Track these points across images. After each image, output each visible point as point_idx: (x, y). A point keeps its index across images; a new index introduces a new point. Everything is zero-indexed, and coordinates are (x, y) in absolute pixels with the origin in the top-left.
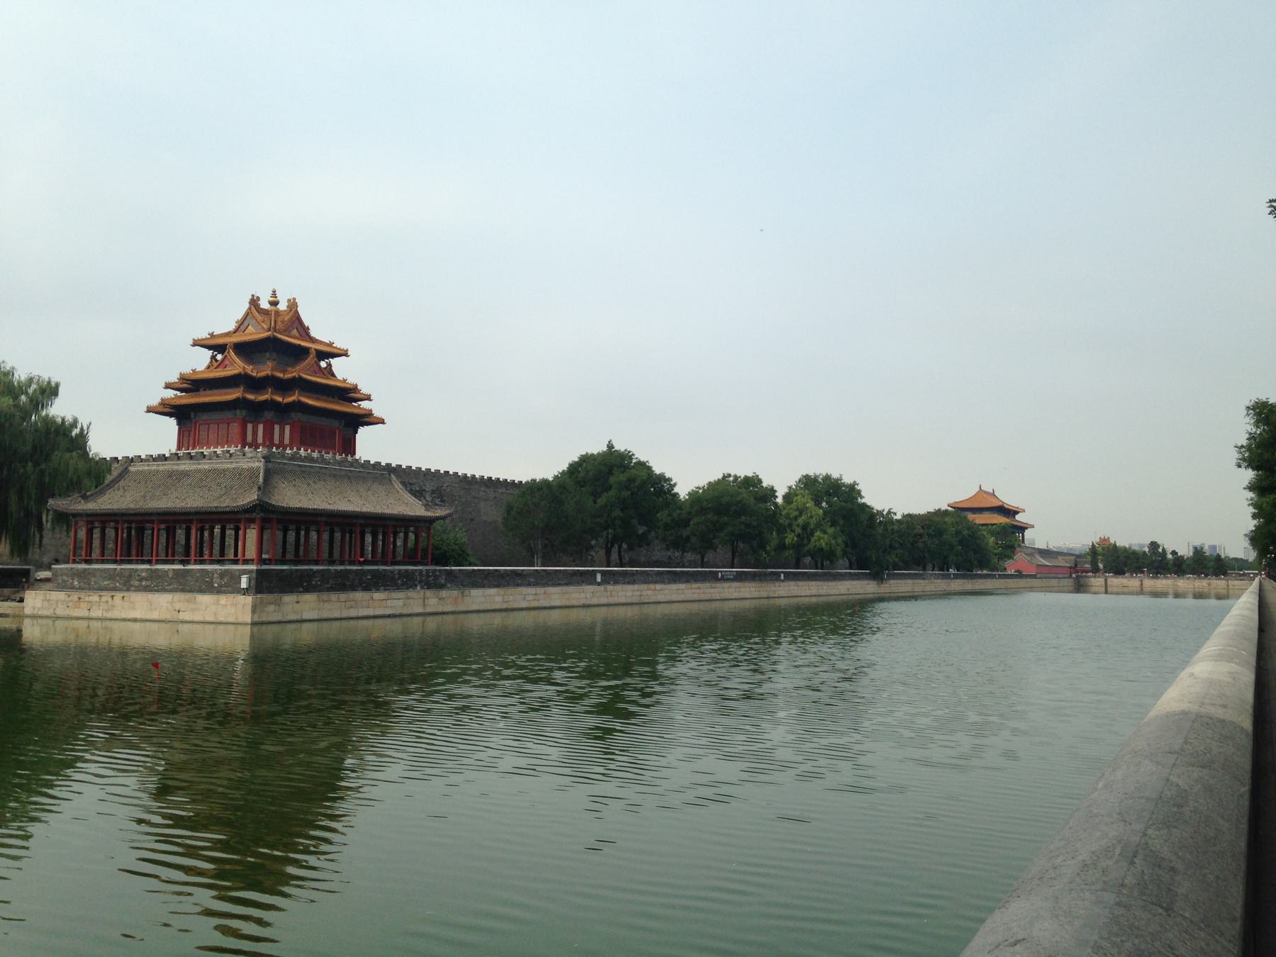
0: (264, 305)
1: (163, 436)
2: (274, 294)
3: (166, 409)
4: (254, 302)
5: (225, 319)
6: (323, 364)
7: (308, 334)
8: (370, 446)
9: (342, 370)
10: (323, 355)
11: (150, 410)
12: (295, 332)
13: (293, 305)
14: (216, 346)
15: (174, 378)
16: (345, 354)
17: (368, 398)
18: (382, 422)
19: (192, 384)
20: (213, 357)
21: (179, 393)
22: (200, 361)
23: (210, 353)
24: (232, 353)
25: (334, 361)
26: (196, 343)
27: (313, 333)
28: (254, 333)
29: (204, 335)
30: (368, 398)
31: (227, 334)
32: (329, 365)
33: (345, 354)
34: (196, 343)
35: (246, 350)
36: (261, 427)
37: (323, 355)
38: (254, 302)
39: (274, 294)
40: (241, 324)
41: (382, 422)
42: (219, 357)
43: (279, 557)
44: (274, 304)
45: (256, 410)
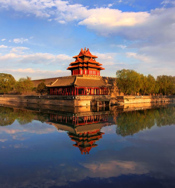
1: (69, 73)
3: (69, 69)
4: (82, 49)
5: (77, 54)
6: (94, 59)
7: (91, 55)
8: (103, 74)
9: (97, 61)
10: (93, 58)
11: (67, 69)
12: (89, 54)
13: (88, 49)
14: (76, 58)
15: (70, 64)
17: (102, 65)
18: (104, 69)
19: (72, 64)
20: (76, 60)
21: (71, 66)
22: (74, 61)
25: (95, 59)
27: (92, 54)
29: (74, 56)
30: (102, 65)
31: (78, 56)
32: (95, 59)
37: (93, 58)
39: (85, 48)
41: (104, 69)
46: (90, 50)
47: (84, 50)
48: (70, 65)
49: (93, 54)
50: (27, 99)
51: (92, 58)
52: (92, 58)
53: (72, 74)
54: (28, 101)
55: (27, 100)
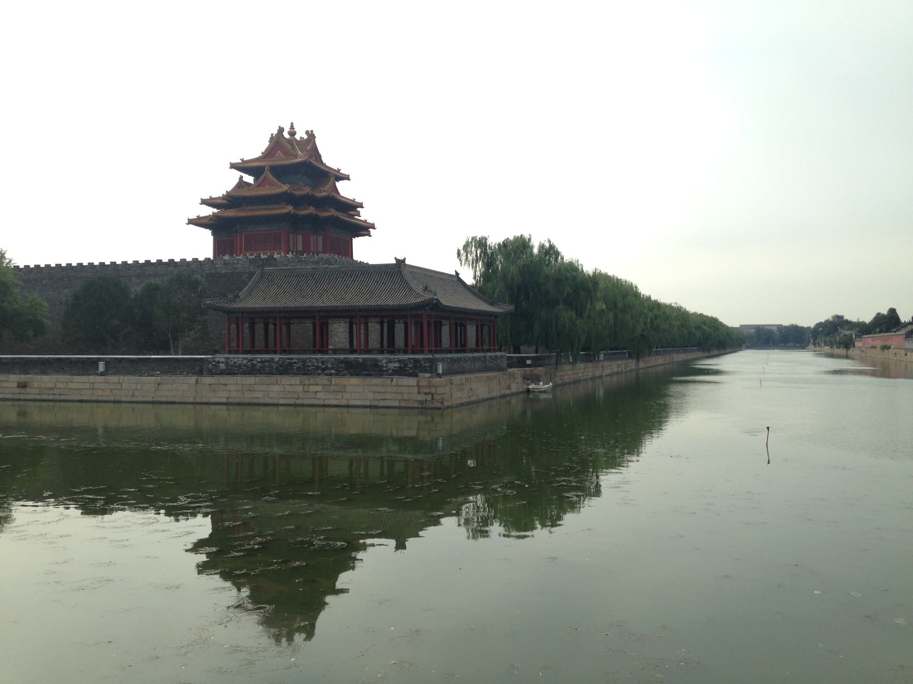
0: (286, 135)
1: (200, 246)
2: (292, 127)
4: (281, 130)
5: (255, 147)
9: (344, 189)
11: (191, 222)
13: (311, 136)
16: (347, 178)
20: (241, 178)
21: (215, 210)
23: (239, 174)
24: (270, 176)
26: (233, 166)
28: (281, 160)
29: (237, 160)
33: (347, 178)
34: (233, 166)
35: (281, 172)
36: (300, 238)
38: (281, 130)
39: (292, 127)
40: (269, 153)
42: (249, 179)
43: (348, 347)
44: (292, 133)
45: (295, 222)
46: (318, 141)
47: (286, 135)
48: (204, 202)
49: (330, 159)
50: (13, 379)
51: (332, 179)
52: (332, 179)
53: (219, 247)
54: (28, 390)
55: (23, 385)
